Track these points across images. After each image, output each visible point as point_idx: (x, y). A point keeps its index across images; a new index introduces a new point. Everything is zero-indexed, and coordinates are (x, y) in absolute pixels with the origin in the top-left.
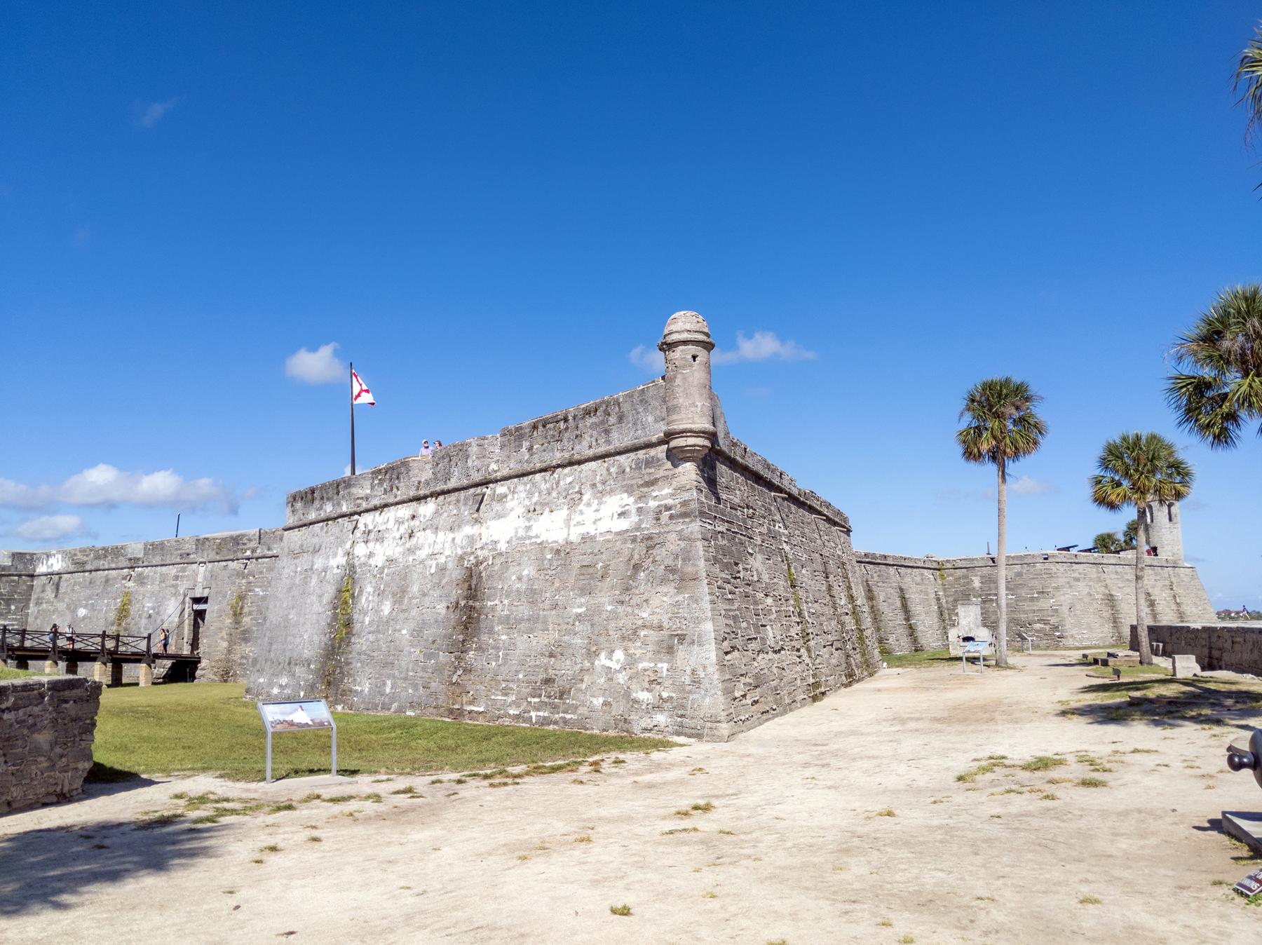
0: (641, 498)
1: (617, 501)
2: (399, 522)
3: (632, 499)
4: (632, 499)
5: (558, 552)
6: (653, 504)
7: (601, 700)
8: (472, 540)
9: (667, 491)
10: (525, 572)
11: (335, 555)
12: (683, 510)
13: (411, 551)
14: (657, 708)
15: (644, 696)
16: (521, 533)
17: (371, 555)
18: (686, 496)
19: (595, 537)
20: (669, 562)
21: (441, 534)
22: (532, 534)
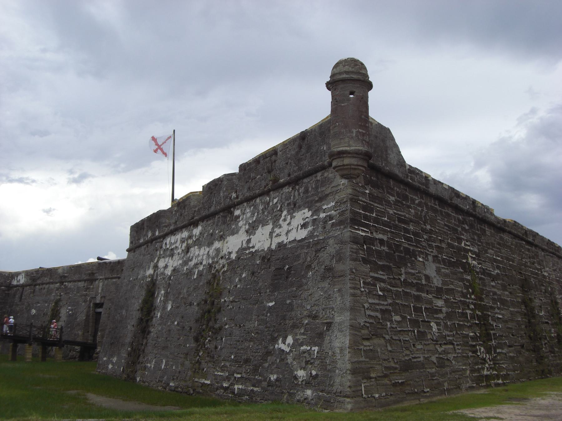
0: (316, 212)
3: (310, 213)
5: (263, 258)
6: (322, 215)
7: (275, 376)
9: (333, 204)
10: (244, 275)
11: (149, 269)
12: (342, 218)
13: (186, 263)
14: (308, 384)
15: (301, 373)
17: (166, 267)
18: (343, 208)
19: (286, 244)
20: (327, 263)
21: (202, 249)
22: (251, 245)
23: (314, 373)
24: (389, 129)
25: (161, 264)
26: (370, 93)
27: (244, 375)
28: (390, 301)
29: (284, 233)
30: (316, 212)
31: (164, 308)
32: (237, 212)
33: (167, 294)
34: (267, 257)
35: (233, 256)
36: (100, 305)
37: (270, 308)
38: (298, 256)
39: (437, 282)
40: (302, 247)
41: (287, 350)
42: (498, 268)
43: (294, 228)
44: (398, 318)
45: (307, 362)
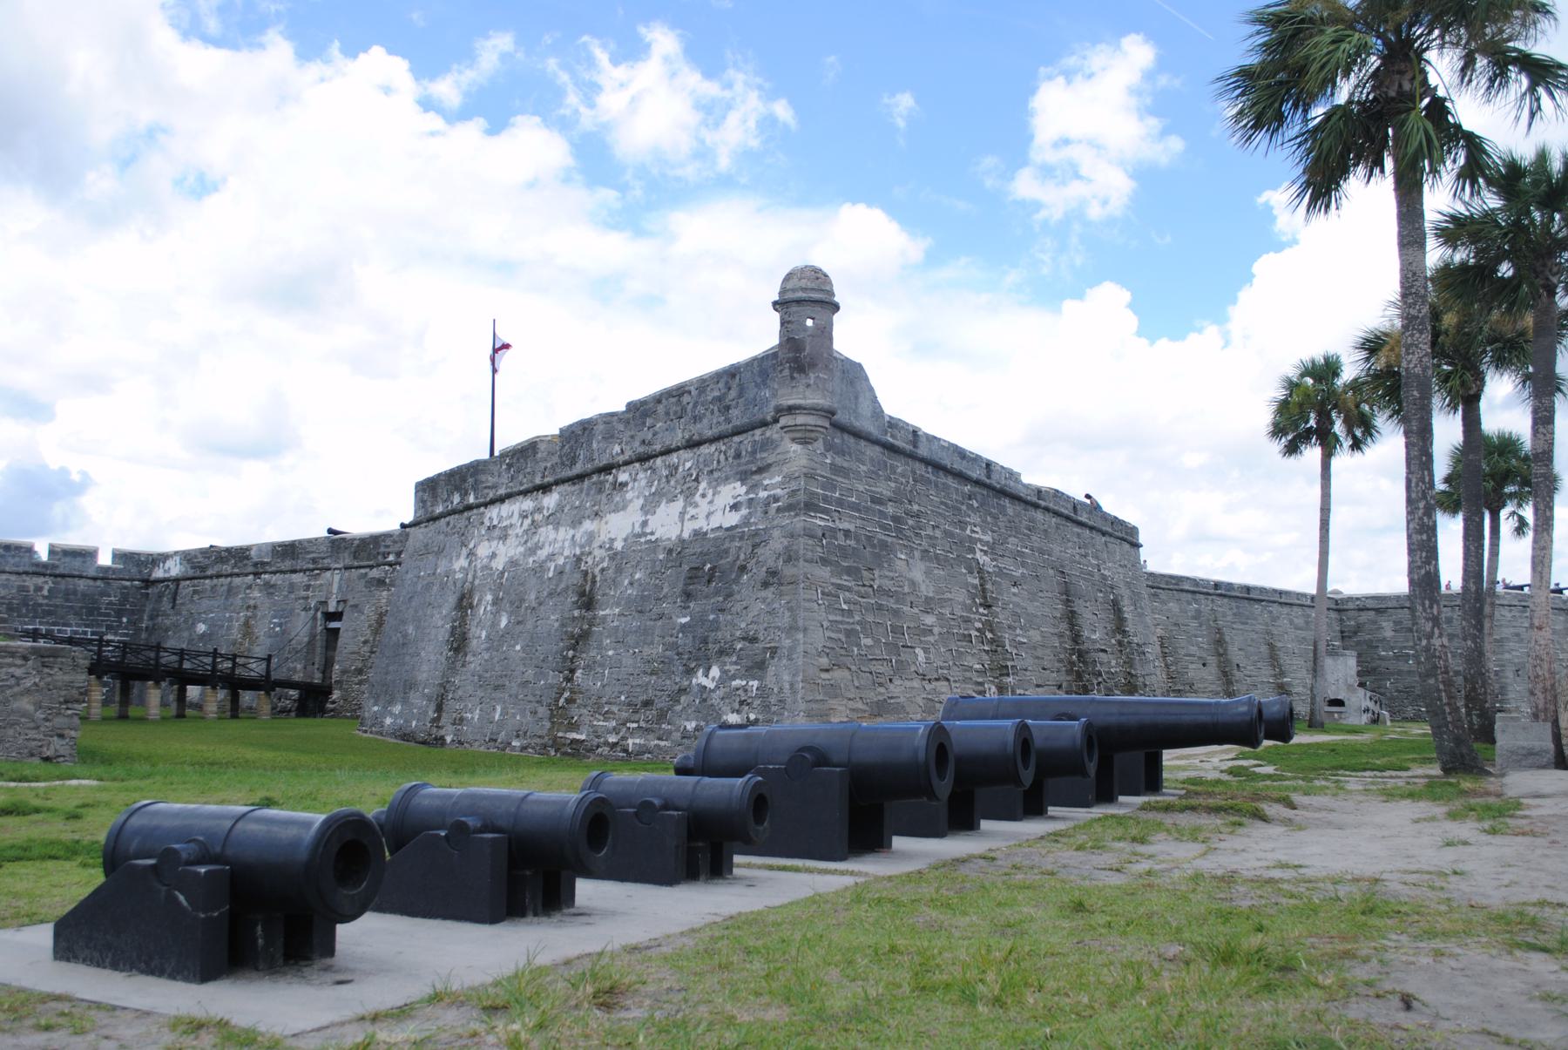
0: (753, 488)
1: (735, 490)
2: (524, 516)
3: (744, 489)
4: (744, 489)
5: (670, 551)
6: (763, 494)
7: (694, 724)
8: (591, 536)
9: (778, 479)
11: (458, 557)
12: (792, 500)
13: (532, 551)
16: (638, 529)
17: (494, 556)
18: (794, 485)
20: (771, 563)
21: (562, 530)
22: (648, 530)
23: (752, 717)
24: (860, 365)
25: (483, 550)
26: (836, 317)
27: (643, 724)
28: (857, 618)
29: (702, 516)
30: (753, 488)
31: (495, 624)
32: (623, 477)
33: (496, 602)
34: (677, 551)
35: (619, 545)
36: (337, 616)
37: (683, 626)
38: (726, 551)
39: (927, 589)
40: (732, 538)
41: (712, 685)
42: (1023, 564)
43: (717, 508)
44: (869, 642)
45: (742, 703)
